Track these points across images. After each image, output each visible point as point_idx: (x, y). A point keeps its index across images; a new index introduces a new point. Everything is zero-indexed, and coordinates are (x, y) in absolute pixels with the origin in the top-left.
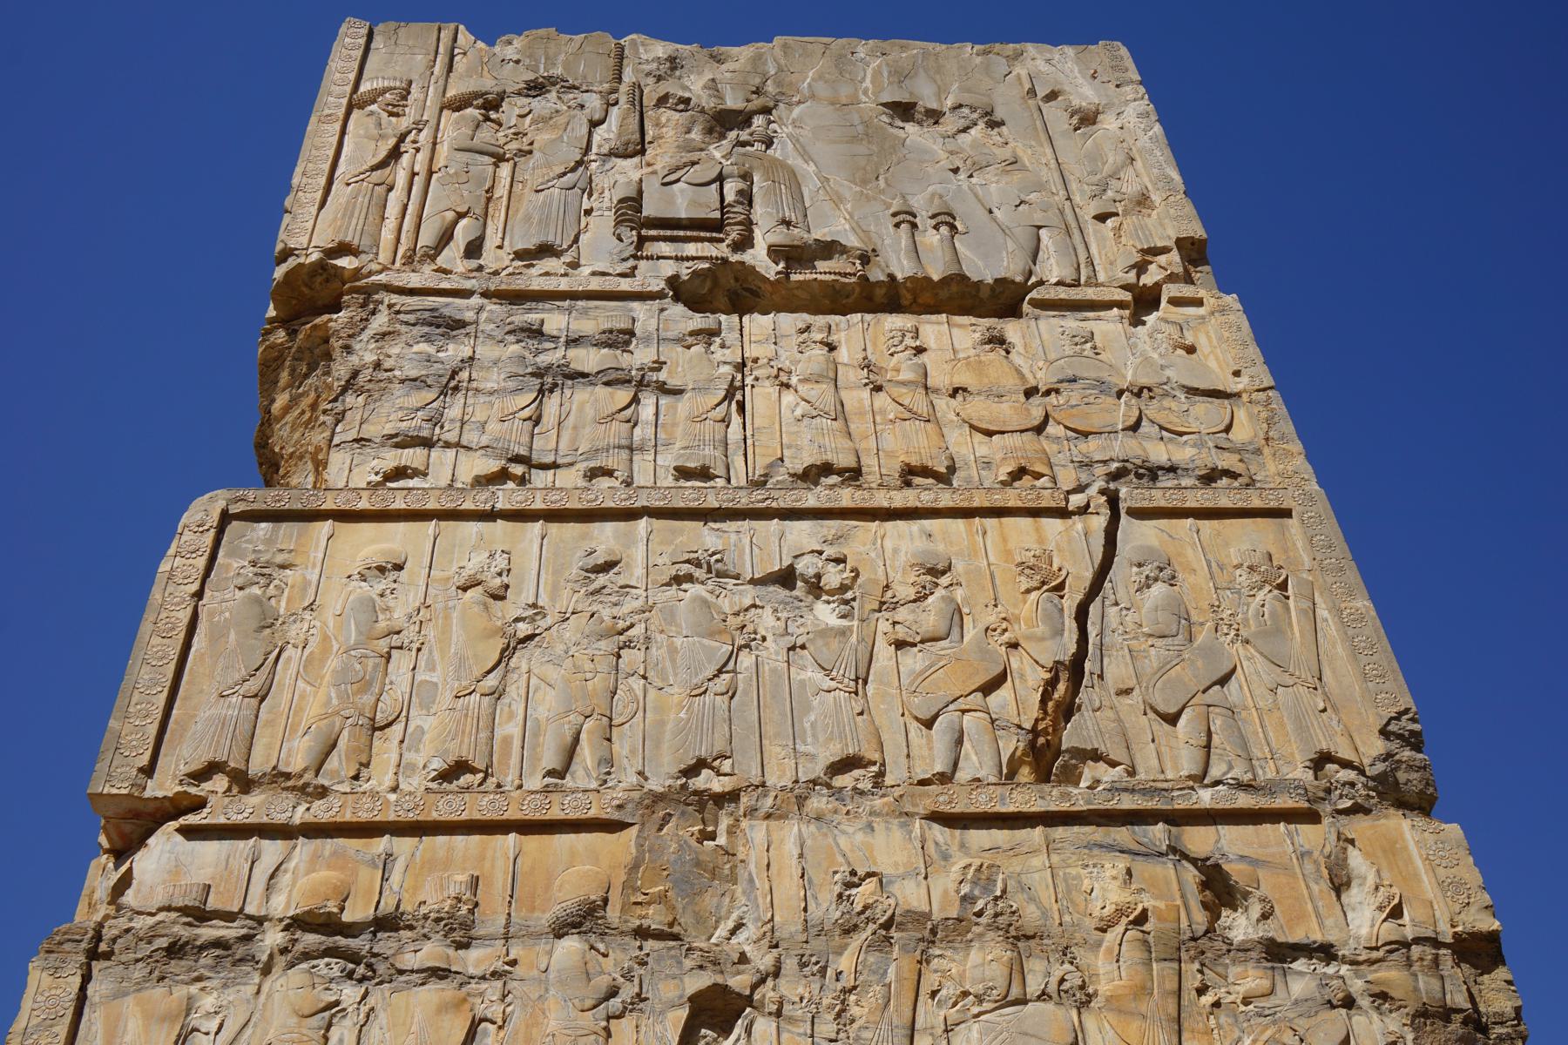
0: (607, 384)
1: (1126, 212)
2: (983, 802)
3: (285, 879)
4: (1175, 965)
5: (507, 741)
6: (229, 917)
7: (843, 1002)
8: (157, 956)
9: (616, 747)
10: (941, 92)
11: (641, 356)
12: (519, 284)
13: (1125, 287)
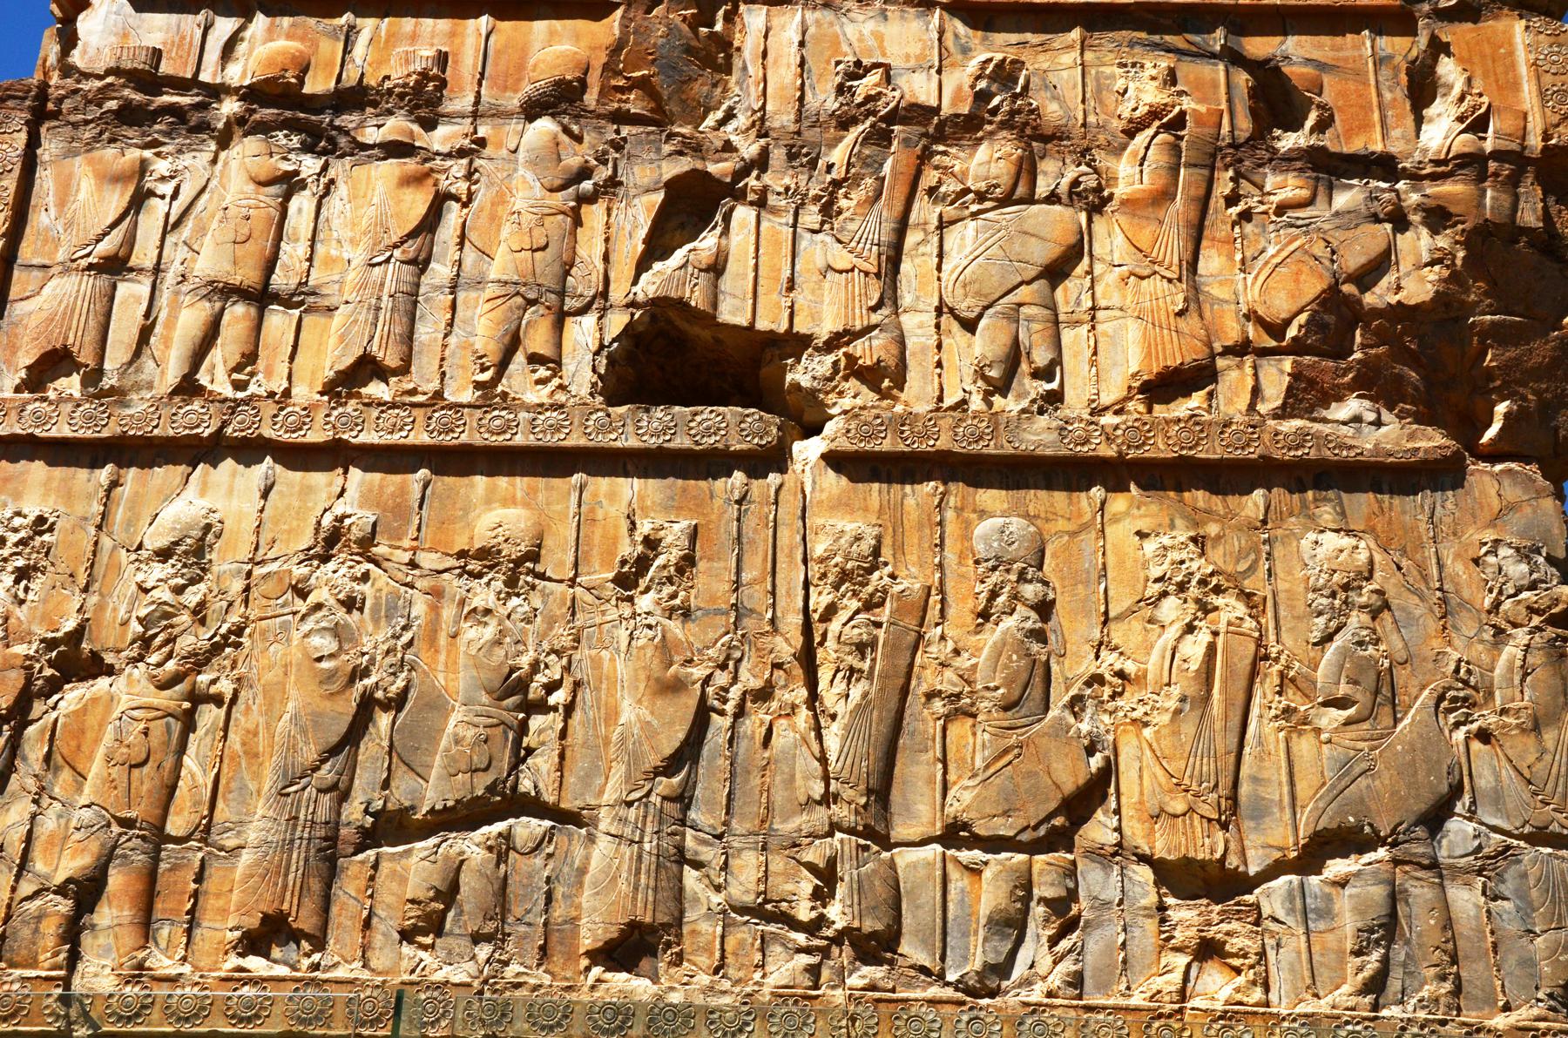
3: (242, 48)
4: (1206, 172)
7: (831, 194)
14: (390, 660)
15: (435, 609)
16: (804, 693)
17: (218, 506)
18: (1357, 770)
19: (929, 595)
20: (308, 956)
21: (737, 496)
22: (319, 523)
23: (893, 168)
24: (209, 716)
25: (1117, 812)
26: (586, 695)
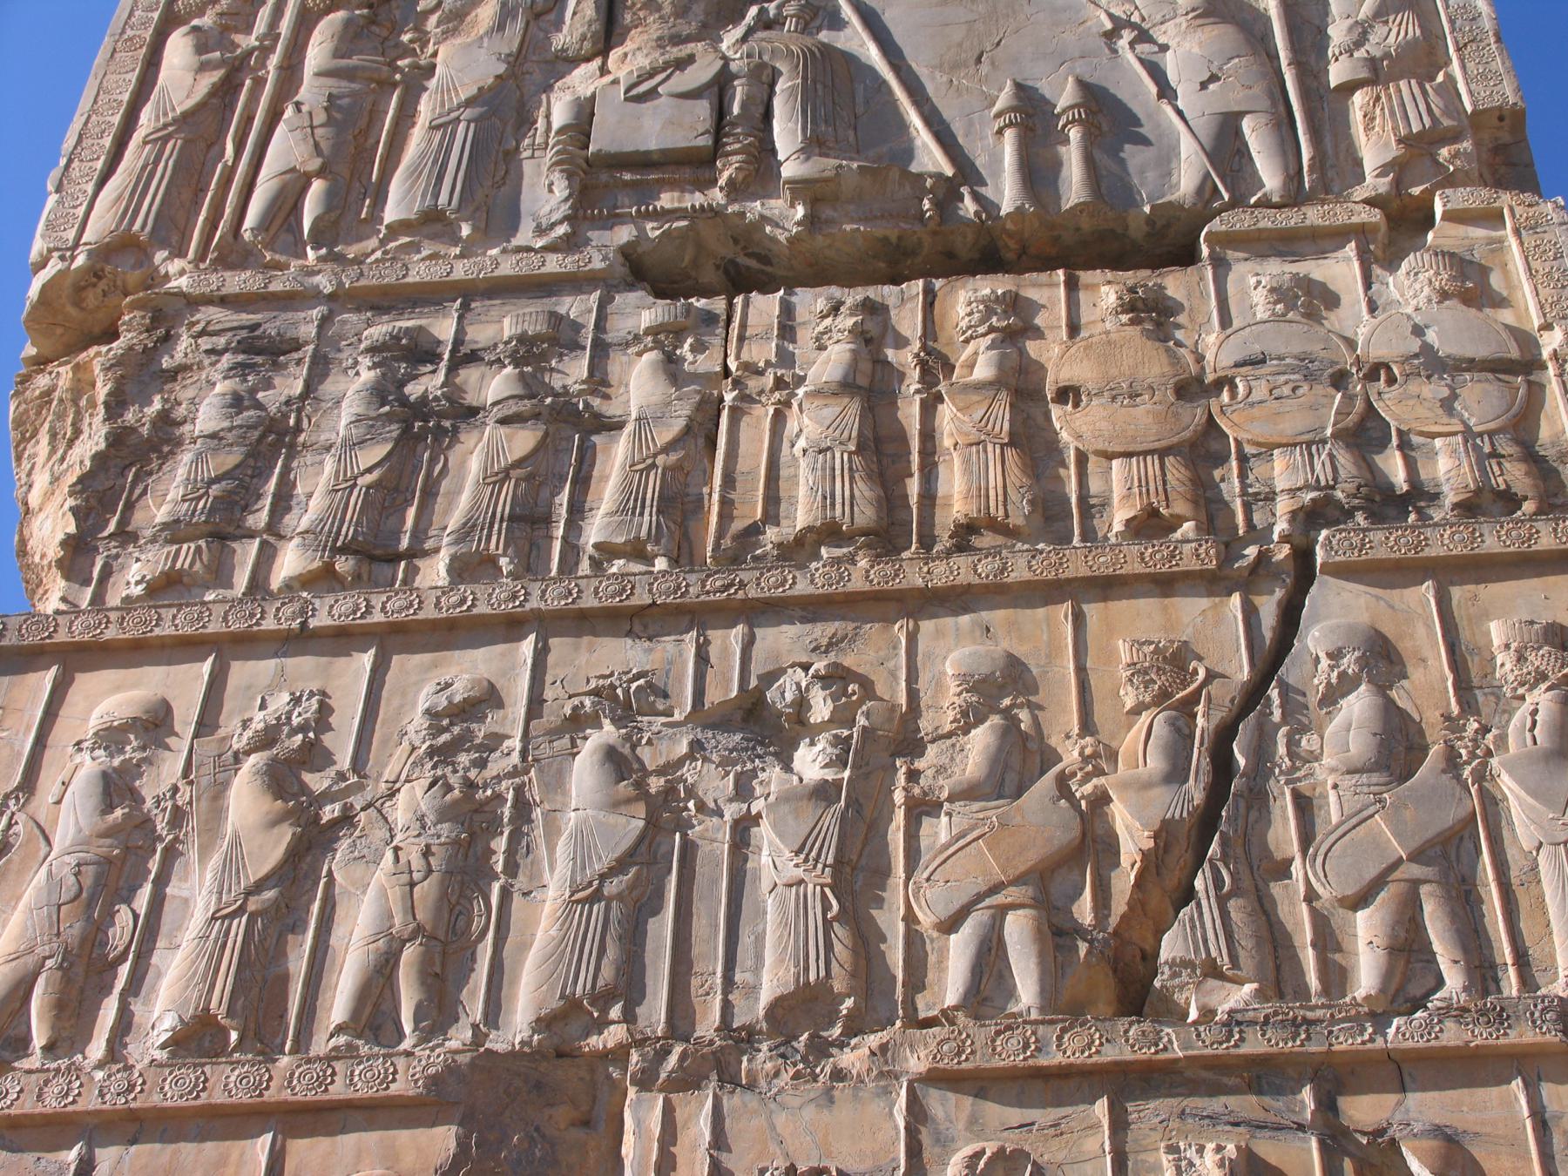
0: (503, 421)
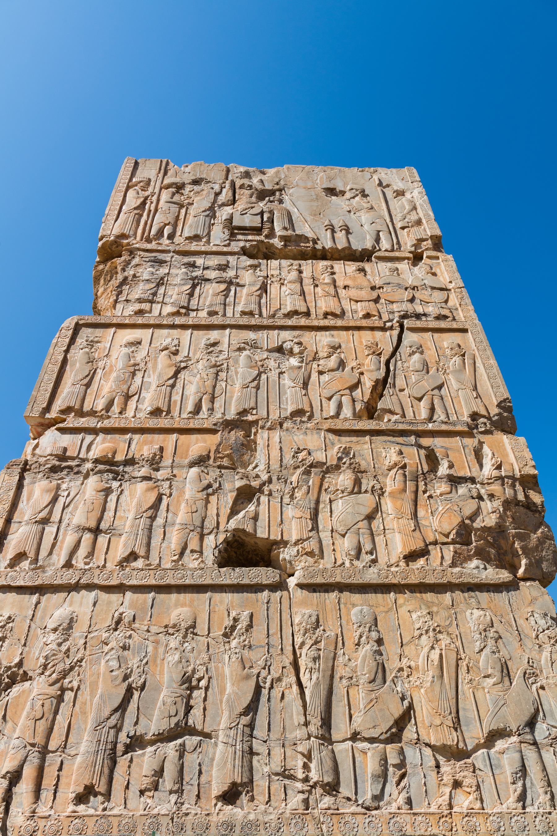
0: (217, 282)
1: (412, 226)
2: (347, 426)
3: (94, 447)
5: (175, 402)
6: (73, 459)
8: (47, 470)
9: (215, 405)
10: (345, 184)
11: (231, 273)
12: (187, 248)
13: (410, 252)
14: (138, 670)
15: (156, 649)
16: (293, 679)
17: (76, 610)
18: (501, 704)
19: (337, 637)
20: (103, 803)
21: (266, 601)
22: (113, 616)
23: (313, 482)
24: (69, 696)
25: (416, 724)
26: (214, 682)
